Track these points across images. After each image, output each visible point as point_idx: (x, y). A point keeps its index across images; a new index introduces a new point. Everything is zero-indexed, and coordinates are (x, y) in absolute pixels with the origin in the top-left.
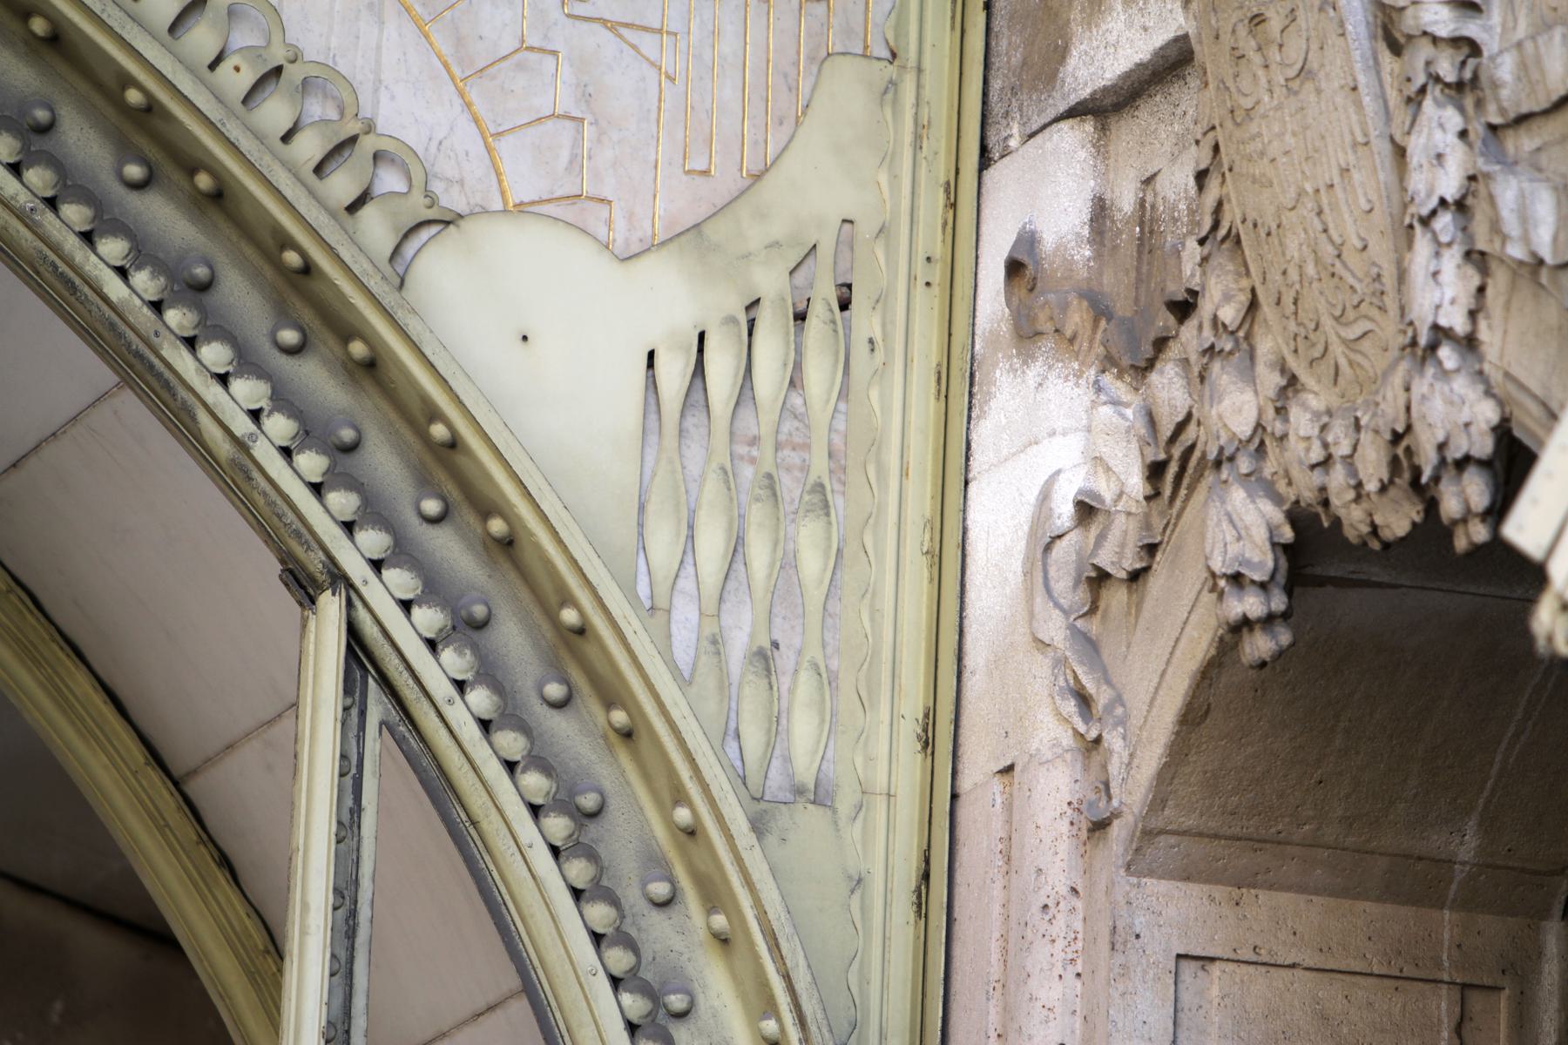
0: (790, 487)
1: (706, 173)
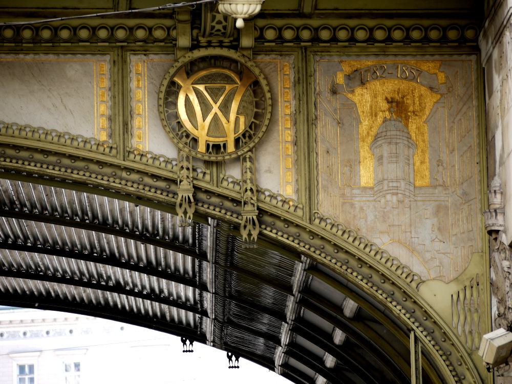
0: (473, 309)
1: (458, 271)
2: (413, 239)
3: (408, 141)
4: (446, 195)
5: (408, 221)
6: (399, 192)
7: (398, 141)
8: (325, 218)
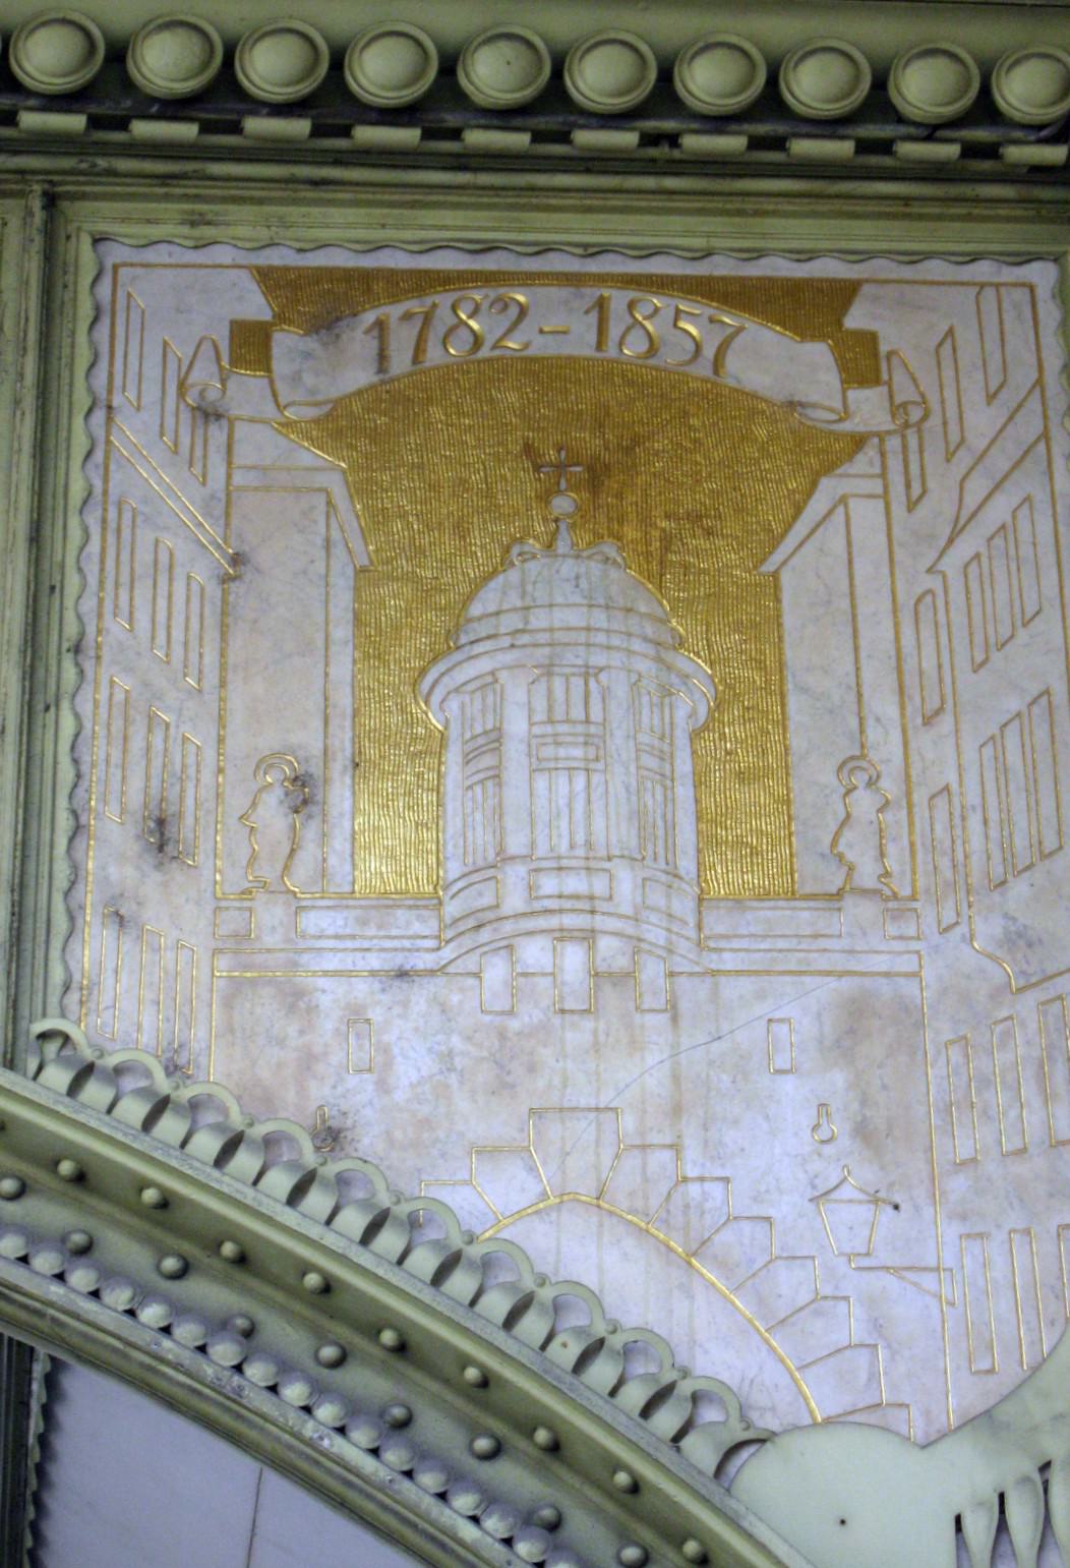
1: (991, 1371)
2: (694, 1190)
3: (659, 660)
4: (898, 946)
5: (656, 1082)
6: (599, 922)
7: (598, 659)
8: (112, 1061)
